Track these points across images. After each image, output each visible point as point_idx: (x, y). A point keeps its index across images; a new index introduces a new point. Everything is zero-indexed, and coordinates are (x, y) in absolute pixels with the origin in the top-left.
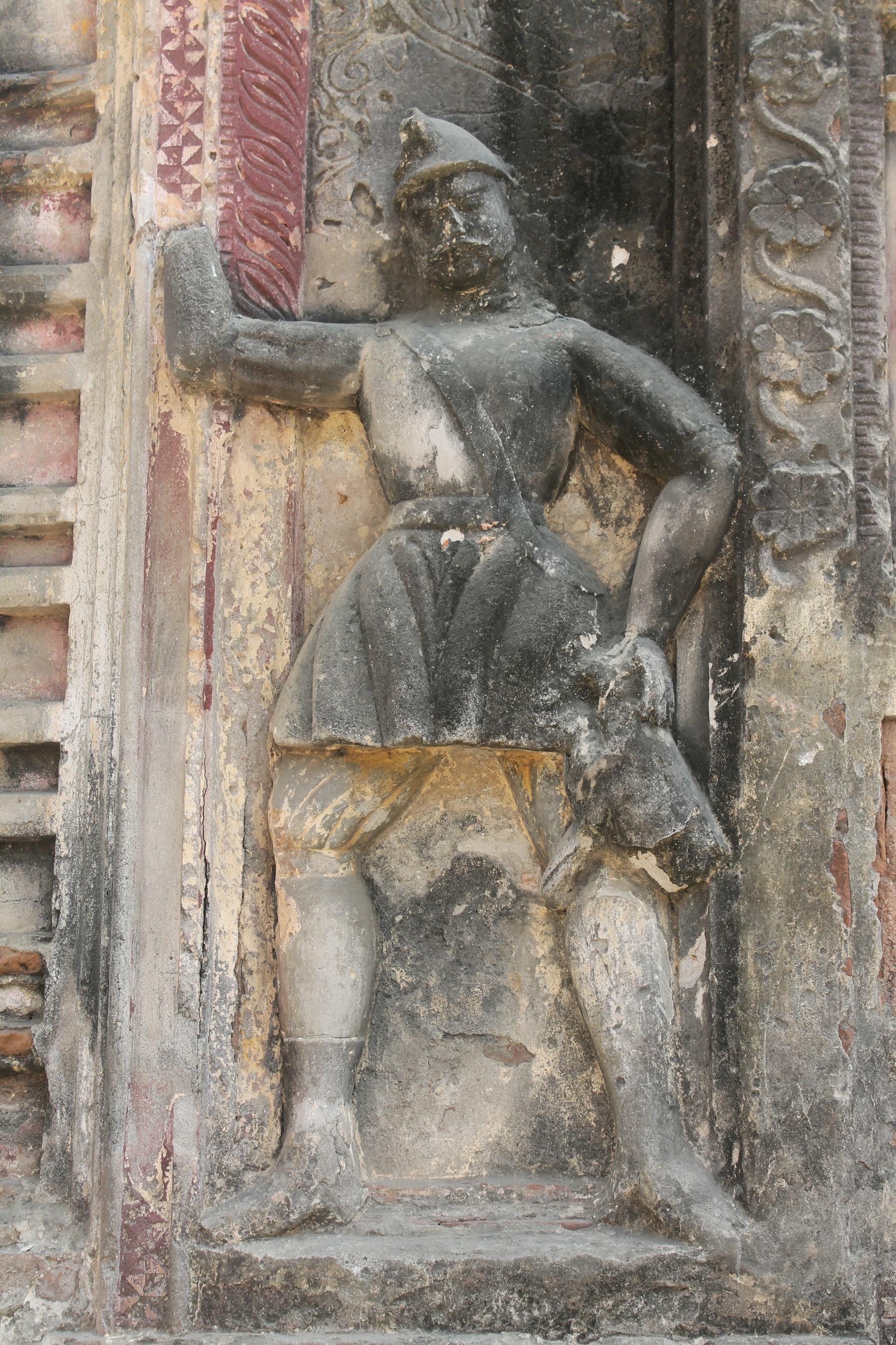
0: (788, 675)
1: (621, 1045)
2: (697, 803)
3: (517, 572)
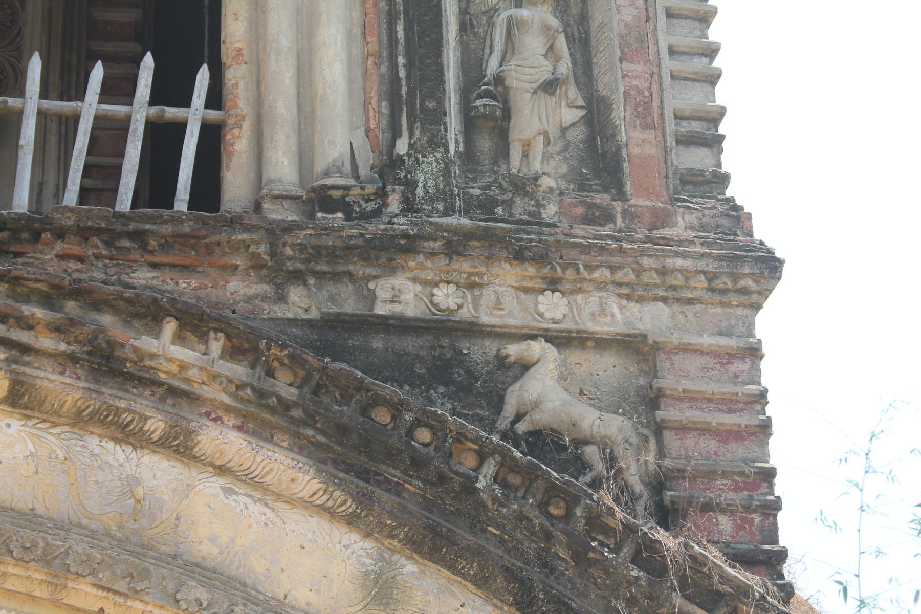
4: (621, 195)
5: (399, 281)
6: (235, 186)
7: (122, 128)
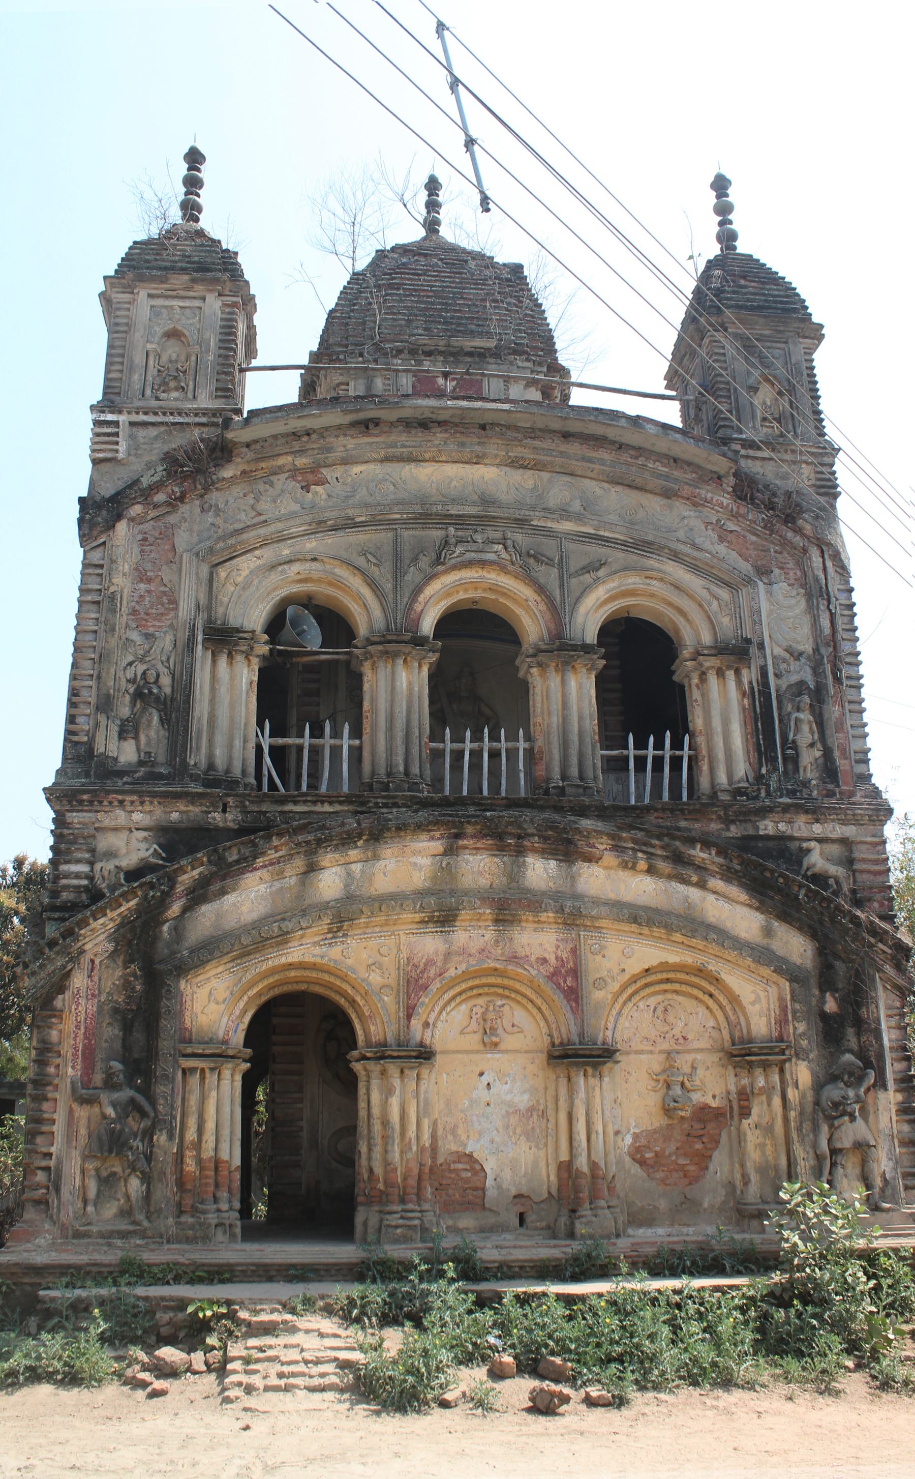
0: (159, 1147)
1: (133, 1199)
2: (146, 1165)
3: (122, 1131)
4: (838, 786)
5: (767, 822)
6: (704, 782)
7: (662, 758)
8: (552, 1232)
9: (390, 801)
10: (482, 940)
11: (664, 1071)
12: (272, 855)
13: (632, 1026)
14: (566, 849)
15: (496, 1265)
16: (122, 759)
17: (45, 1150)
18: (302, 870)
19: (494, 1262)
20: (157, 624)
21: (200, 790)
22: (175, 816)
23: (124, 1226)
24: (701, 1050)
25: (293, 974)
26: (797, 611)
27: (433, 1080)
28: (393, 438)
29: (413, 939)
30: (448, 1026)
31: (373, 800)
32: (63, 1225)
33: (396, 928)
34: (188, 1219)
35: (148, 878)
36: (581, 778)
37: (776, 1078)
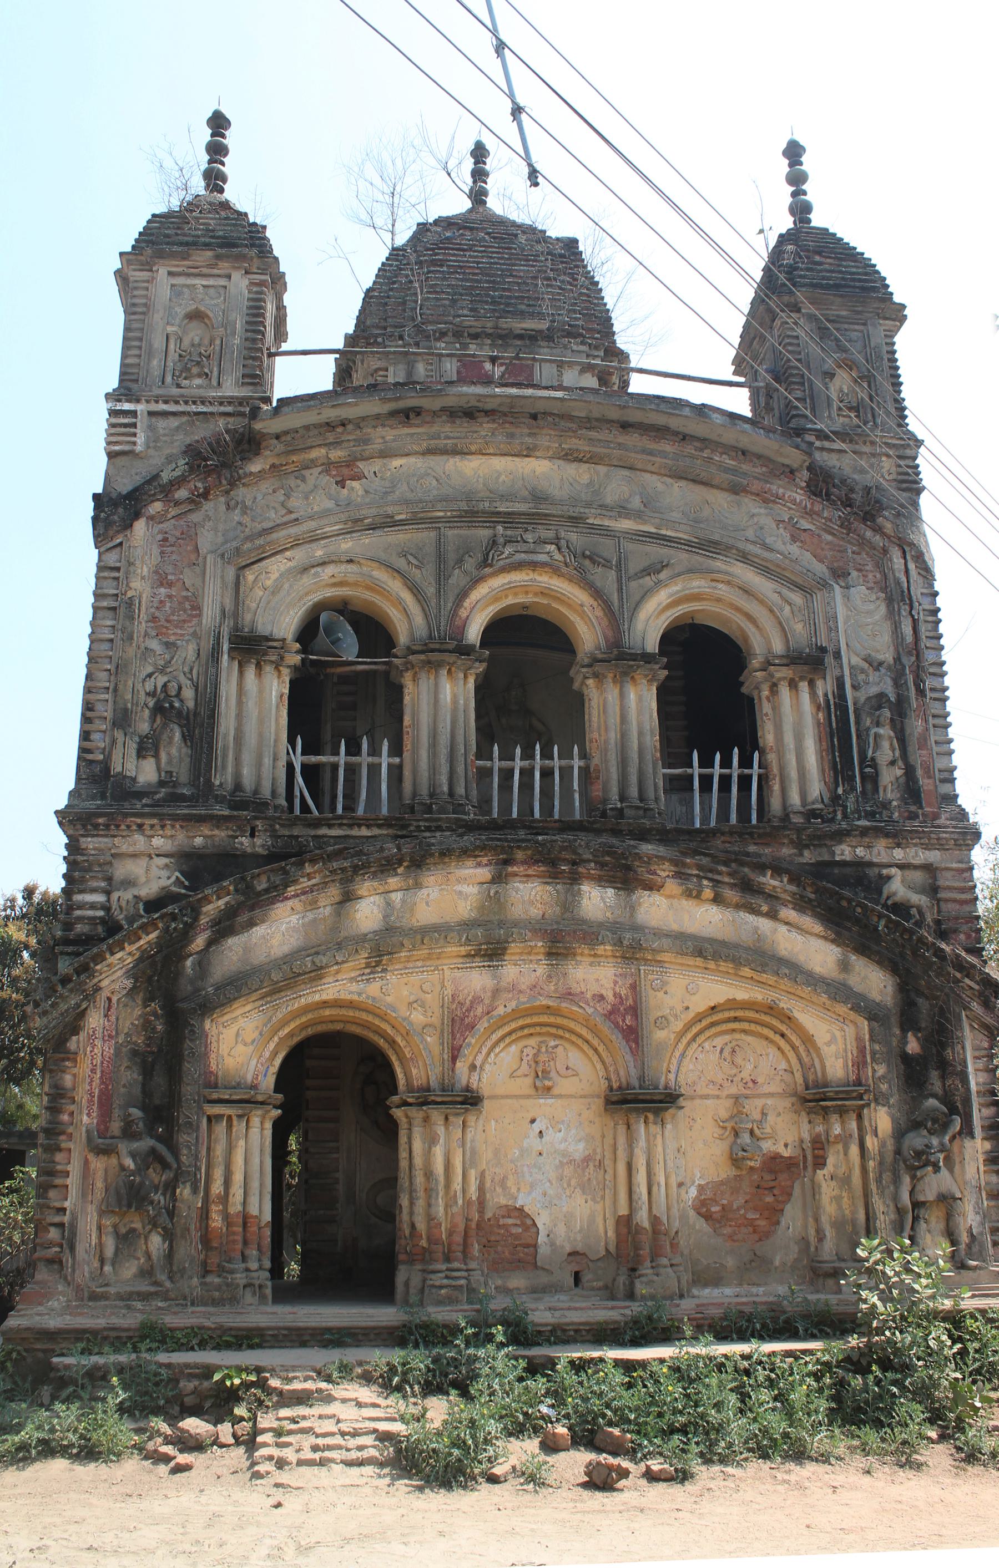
1: (154, 1257)
2: (168, 1221)
3: (142, 1184)
4: (921, 807)
5: (844, 847)
6: (775, 804)
7: (729, 777)
8: (610, 1293)
9: (434, 824)
10: (533, 975)
11: (732, 1117)
12: (305, 883)
13: (697, 1068)
14: (625, 877)
15: (549, 1328)
16: (142, 779)
17: (58, 1205)
18: (337, 899)
19: (547, 1325)
20: (179, 632)
21: (226, 812)
22: (199, 841)
23: (145, 1287)
24: (771, 1095)
25: (327, 1012)
26: (877, 617)
27: (480, 1128)
28: (435, 428)
29: (458, 974)
30: (497, 1068)
31: (415, 823)
32: (78, 1286)
33: (439, 962)
34: (214, 1279)
35: (170, 909)
36: (641, 800)
37: (854, 1125)
